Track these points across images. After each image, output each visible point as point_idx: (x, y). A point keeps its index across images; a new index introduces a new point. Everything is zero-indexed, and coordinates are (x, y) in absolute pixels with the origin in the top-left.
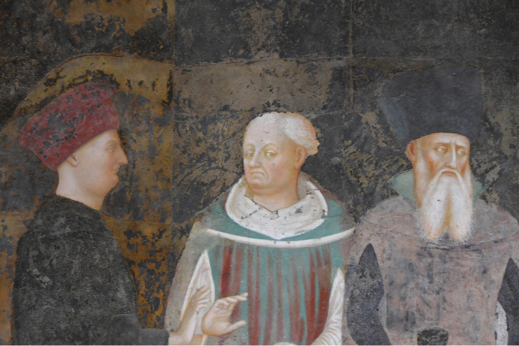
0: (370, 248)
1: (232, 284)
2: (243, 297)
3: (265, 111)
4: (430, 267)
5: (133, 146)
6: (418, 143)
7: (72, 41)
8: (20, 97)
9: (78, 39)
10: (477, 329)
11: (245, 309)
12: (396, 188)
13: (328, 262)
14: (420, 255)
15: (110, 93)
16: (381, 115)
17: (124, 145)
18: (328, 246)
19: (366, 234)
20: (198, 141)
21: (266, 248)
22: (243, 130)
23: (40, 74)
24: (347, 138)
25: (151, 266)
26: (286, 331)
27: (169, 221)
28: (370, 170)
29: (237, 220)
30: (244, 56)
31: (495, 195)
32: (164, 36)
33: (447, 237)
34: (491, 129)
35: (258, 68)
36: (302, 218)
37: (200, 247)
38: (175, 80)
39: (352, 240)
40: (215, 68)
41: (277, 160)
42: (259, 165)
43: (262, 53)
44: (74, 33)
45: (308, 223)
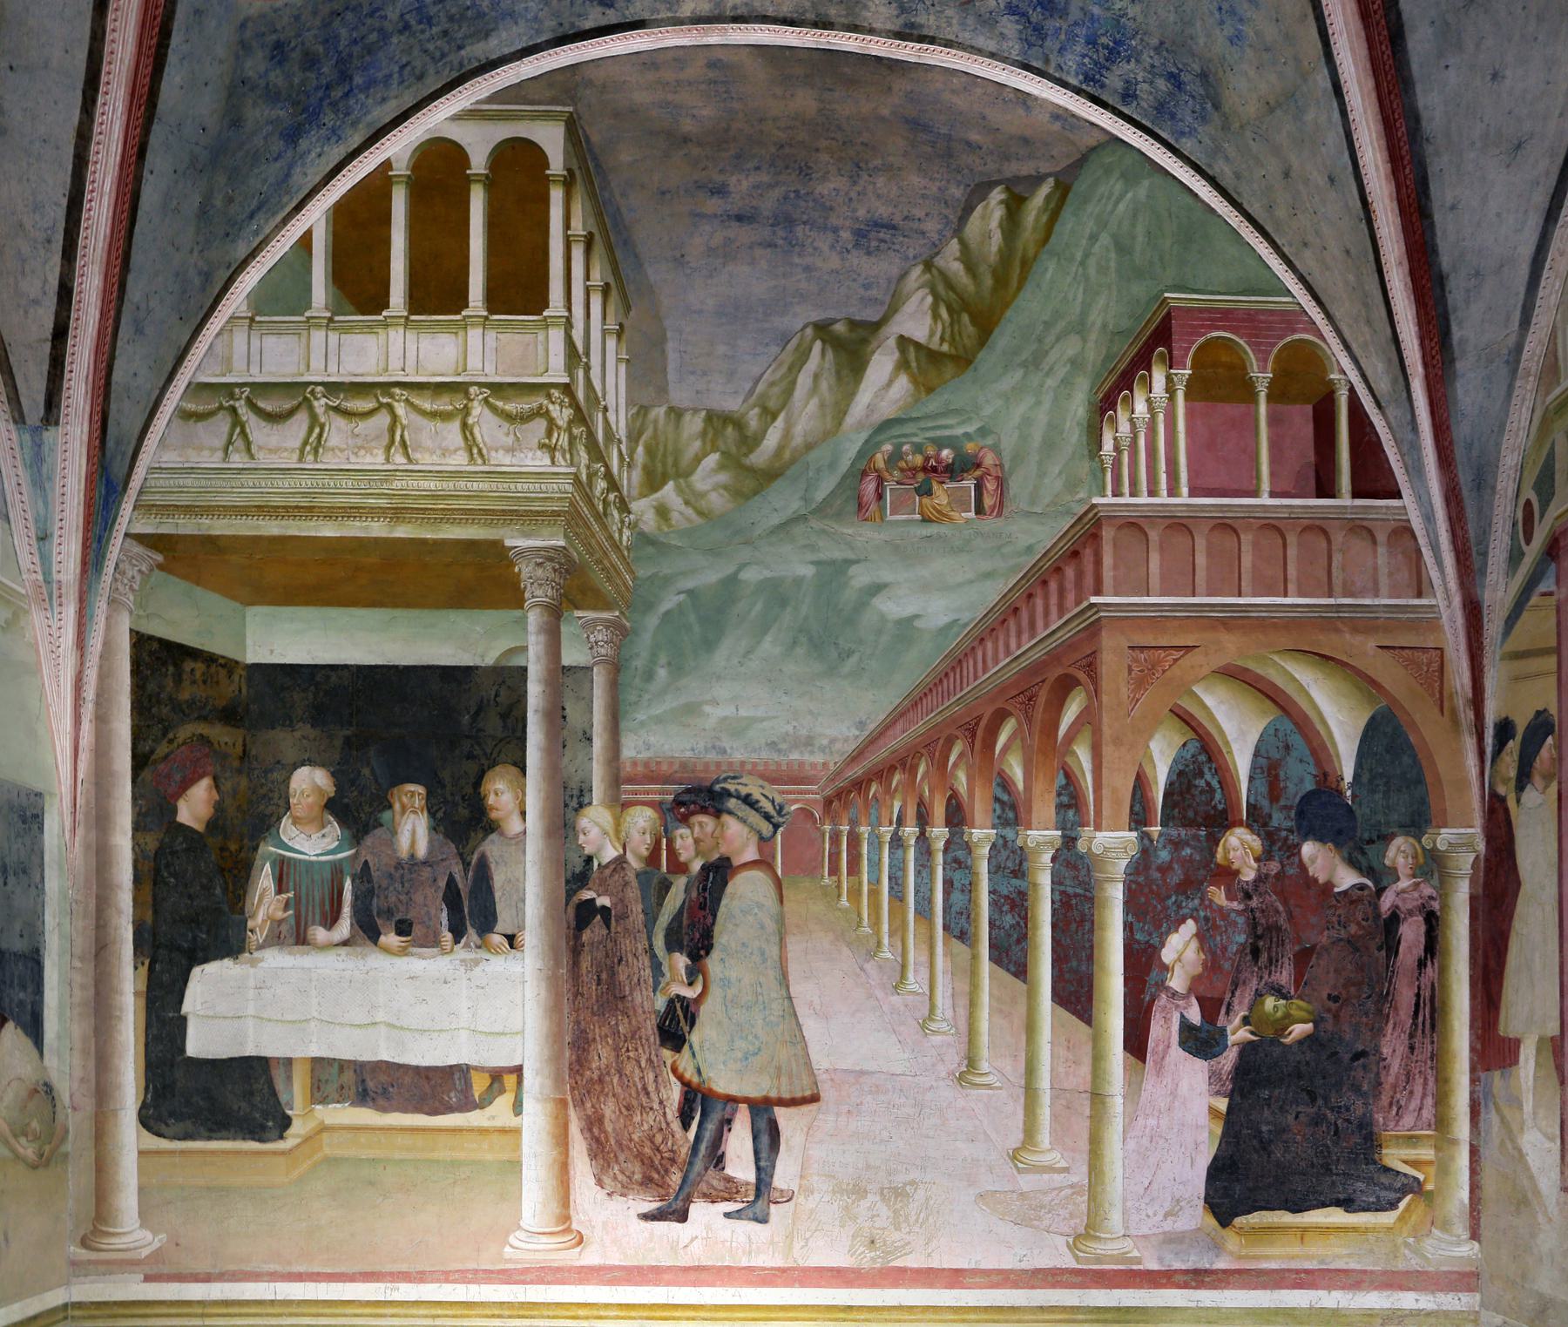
0: (366, 861)
1: (284, 886)
2: (291, 895)
3: (303, 765)
4: (402, 876)
5: (222, 788)
6: (395, 790)
7: (183, 712)
8: (152, 752)
9: (187, 711)
10: (430, 919)
11: (292, 903)
12: (382, 821)
13: (341, 872)
14: (396, 868)
15: (207, 750)
16: (372, 770)
17: (217, 787)
18: (341, 860)
19: (364, 853)
20: (262, 785)
21: (305, 861)
22: (289, 778)
23: (164, 735)
24: (353, 785)
25: (236, 872)
26: (317, 917)
27: (246, 841)
28: (367, 809)
29: (286, 841)
30: (290, 726)
31: (442, 828)
32: (240, 710)
33: (412, 856)
34: (439, 782)
35: (298, 734)
36: (326, 840)
37: (264, 860)
38: (248, 739)
39: (355, 856)
40: (271, 734)
41: (310, 800)
42: (299, 803)
43: (301, 724)
44: (184, 706)
45: (329, 844)
